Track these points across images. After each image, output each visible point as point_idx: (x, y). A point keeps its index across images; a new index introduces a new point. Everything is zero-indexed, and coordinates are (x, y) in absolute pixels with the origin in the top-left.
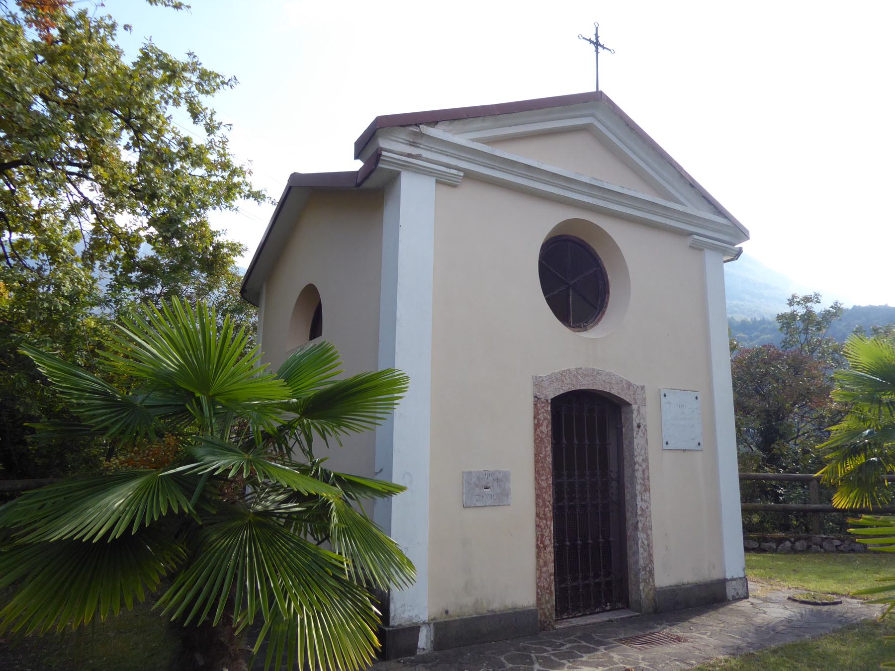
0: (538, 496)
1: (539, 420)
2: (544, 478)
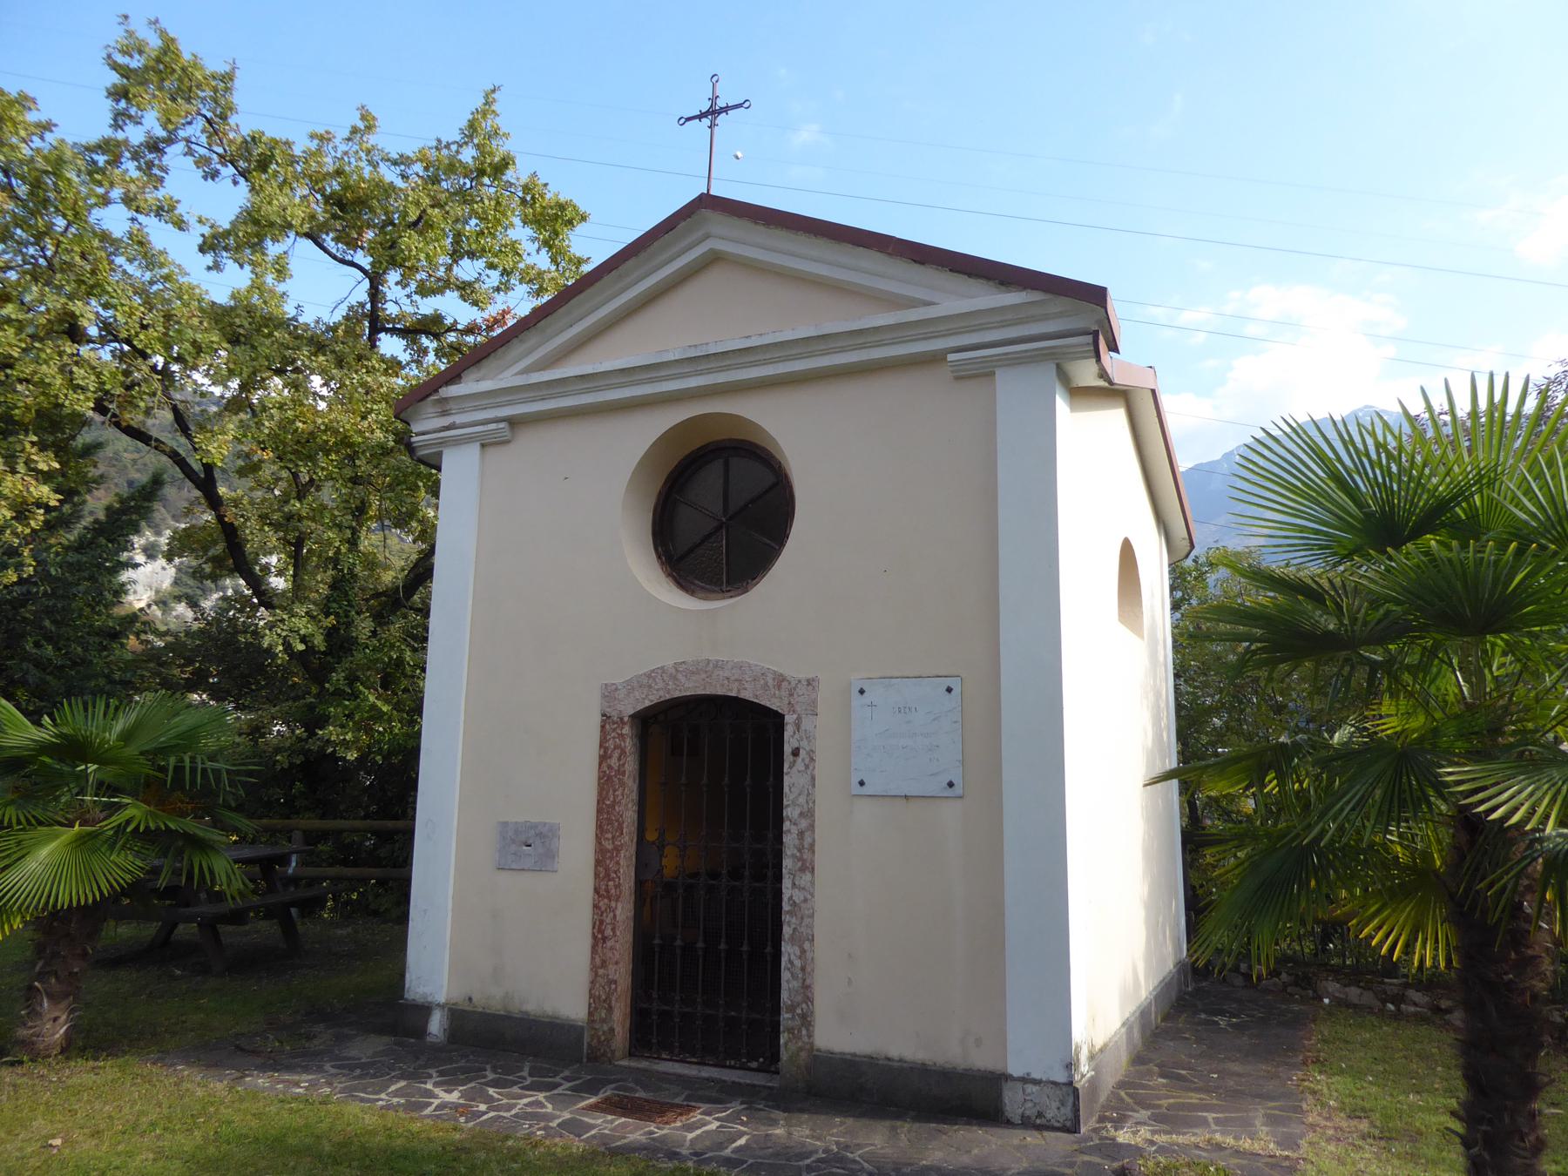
0: (598, 863)
1: (606, 749)
2: (609, 836)
